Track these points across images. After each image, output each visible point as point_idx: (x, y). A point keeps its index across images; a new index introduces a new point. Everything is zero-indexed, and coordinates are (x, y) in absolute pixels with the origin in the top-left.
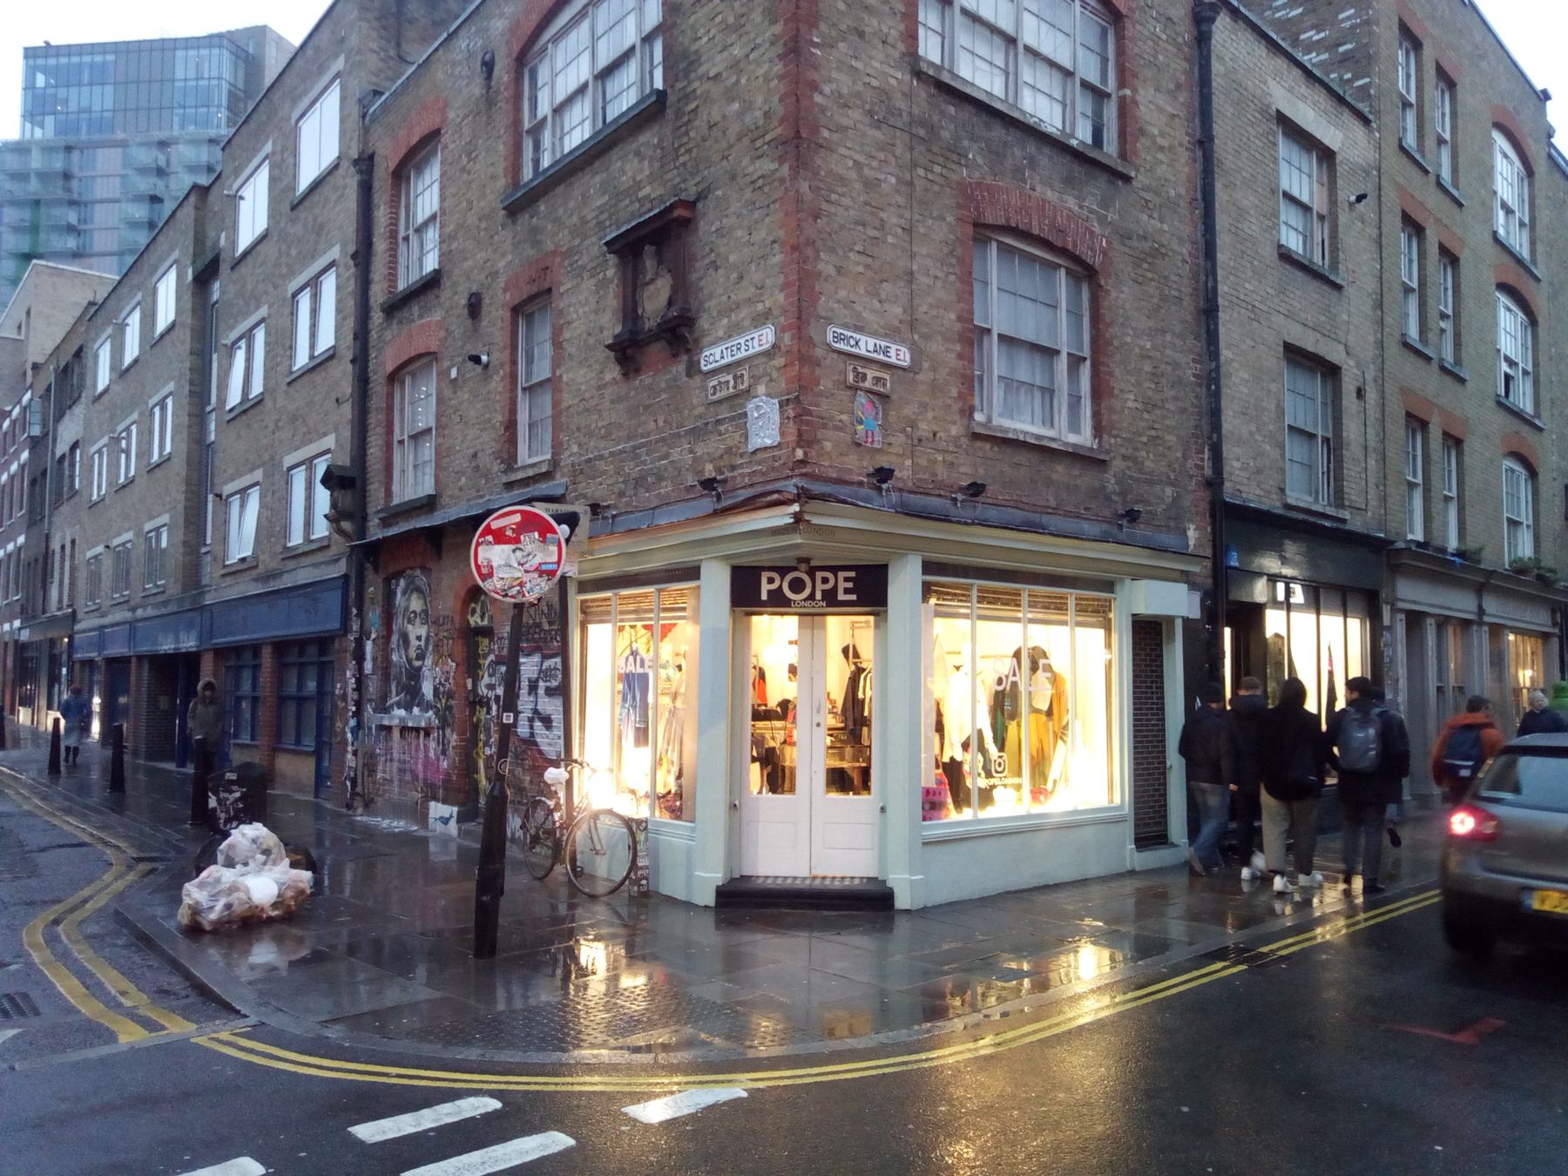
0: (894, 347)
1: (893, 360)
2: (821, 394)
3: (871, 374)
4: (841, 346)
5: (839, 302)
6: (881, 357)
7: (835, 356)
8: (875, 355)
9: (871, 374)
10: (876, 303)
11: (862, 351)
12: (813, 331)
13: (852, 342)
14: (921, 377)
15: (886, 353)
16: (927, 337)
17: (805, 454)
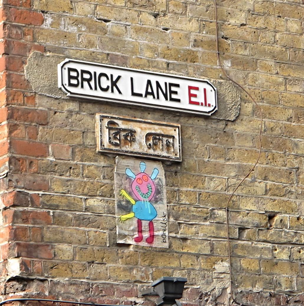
0: (184, 85)
1: (185, 105)
2: (51, 168)
3: (141, 131)
4: (86, 91)
5: (77, 22)
6: (162, 102)
7: (73, 106)
8: (150, 100)
9: (141, 131)
10: (147, 18)
11: (127, 96)
12: (29, 72)
13: (105, 83)
14: (239, 128)
15: (170, 92)
16: (247, 64)
17: (24, 265)
